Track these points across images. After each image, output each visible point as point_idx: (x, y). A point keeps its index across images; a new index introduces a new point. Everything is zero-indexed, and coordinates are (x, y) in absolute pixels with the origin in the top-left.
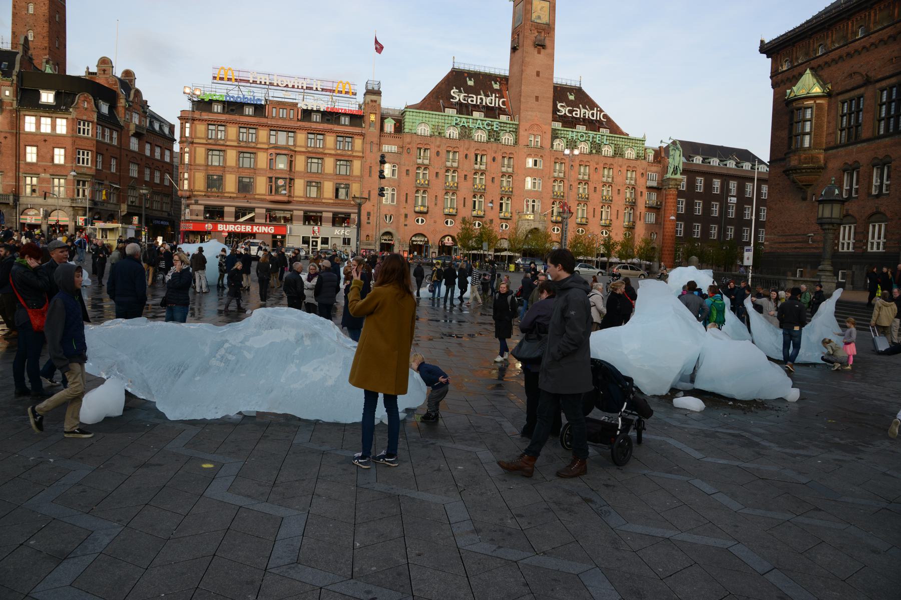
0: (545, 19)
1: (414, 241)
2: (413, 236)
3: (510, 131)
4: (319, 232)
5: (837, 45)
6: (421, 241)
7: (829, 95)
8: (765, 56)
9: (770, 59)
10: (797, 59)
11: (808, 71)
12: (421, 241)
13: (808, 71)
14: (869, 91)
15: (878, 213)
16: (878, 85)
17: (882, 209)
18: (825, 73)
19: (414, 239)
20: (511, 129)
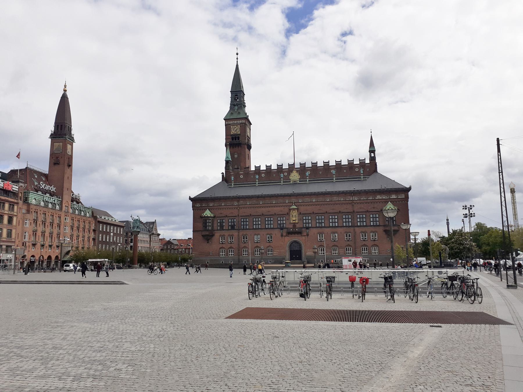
0: (70, 154)
1: (32, 259)
2: (31, 257)
3: (59, 204)
4: (2, 257)
5: (216, 205)
6: (33, 259)
7: (214, 217)
8: (190, 201)
9: (192, 202)
10: (203, 205)
11: (208, 209)
12: (33, 259)
13: (208, 209)
14: (227, 219)
15: (231, 247)
16: (229, 218)
17: (232, 246)
18: (212, 211)
19: (31, 258)
20: (59, 203)
